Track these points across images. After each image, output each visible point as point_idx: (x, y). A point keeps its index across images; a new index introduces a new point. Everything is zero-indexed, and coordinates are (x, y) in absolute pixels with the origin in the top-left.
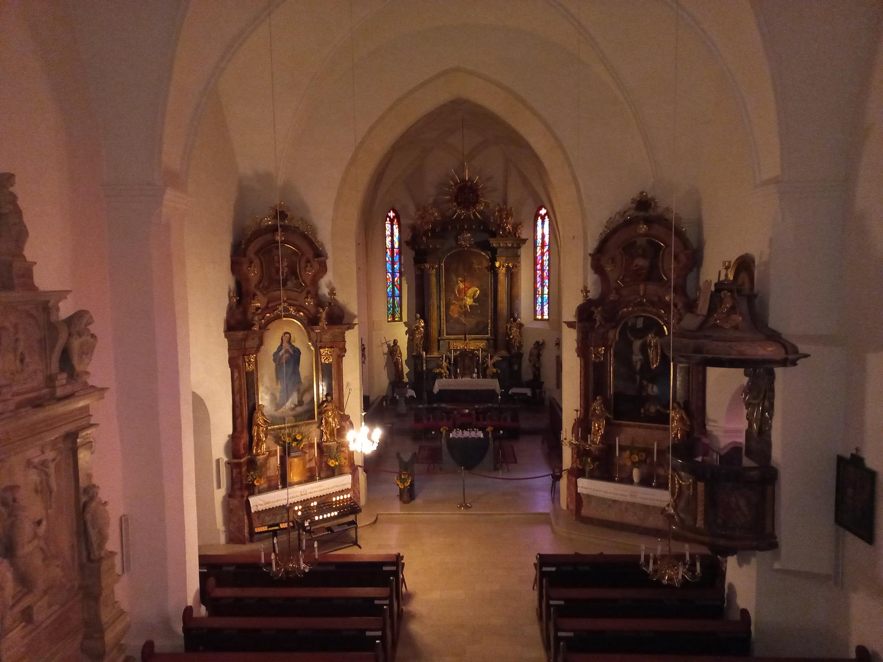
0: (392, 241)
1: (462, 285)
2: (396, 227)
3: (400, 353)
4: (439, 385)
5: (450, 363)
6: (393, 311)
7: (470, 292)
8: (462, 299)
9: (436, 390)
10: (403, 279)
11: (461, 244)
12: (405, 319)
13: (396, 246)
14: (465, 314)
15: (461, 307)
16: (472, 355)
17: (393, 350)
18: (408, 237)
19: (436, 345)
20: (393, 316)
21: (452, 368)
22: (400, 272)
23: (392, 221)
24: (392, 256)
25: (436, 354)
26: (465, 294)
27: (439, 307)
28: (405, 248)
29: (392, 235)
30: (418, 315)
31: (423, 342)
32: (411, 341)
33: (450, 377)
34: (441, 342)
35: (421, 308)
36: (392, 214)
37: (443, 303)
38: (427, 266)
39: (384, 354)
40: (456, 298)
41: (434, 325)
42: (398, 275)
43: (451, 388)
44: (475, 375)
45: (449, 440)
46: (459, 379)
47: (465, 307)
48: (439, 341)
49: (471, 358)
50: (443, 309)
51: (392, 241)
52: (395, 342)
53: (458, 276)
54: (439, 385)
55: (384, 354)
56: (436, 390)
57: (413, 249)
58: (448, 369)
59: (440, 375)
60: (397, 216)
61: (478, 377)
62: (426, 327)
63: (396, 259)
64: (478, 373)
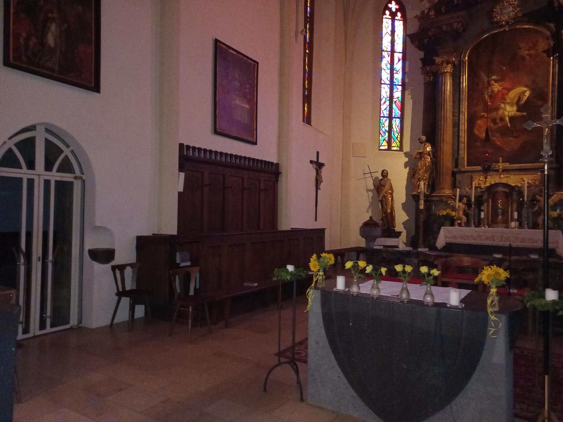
0: (393, 42)
1: (496, 87)
2: (399, 26)
3: (391, 188)
4: (444, 236)
5: (469, 204)
6: (390, 137)
7: (513, 94)
8: (497, 109)
9: (441, 242)
10: (407, 93)
11: (497, 23)
12: (407, 148)
13: (399, 47)
14: (504, 132)
15: (494, 121)
16: (512, 192)
17: (381, 186)
18: (414, 28)
19: (448, 179)
20: (389, 142)
21: (471, 212)
22: (403, 85)
23: (393, 15)
24: (392, 62)
25: (448, 192)
26: (503, 99)
27: (456, 125)
28: (412, 48)
29: (393, 33)
30: (424, 138)
31: (430, 175)
32: (412, 175)
33: (468, 224)
34: (458, 177)
35: (430, 129)
36: (393, 6)
37: (464, 118)
38: (438, 60)
39: (368, 190)
40: (487, 109)
41: (447, 148)
42: (400, 88)
43: (467, 241)
44: (513, 224)
45: (328, 296)
46: (484, 229)
47: (502, 119)
48: (454, 174)
49: (507, 196)
50: (464, 126)
51: (393, 42)
52: (385, 174)
53: (490, 73)
54: (444, 236)
55: (368, 190)
56: (441, 242)
57: (420, 47)
58: (466, 214)
59: (452, 222)
60: (402, 9)
61: (521, 226)
62: (435, 154)
63: (398, 66)
64: (519, 220)
